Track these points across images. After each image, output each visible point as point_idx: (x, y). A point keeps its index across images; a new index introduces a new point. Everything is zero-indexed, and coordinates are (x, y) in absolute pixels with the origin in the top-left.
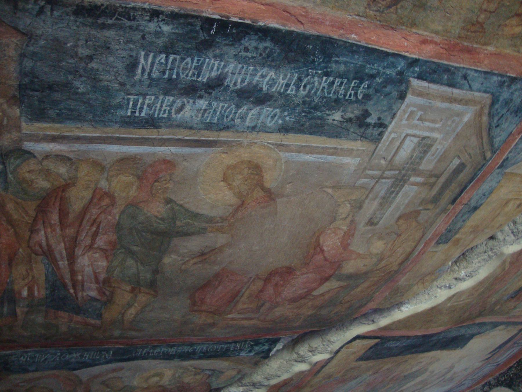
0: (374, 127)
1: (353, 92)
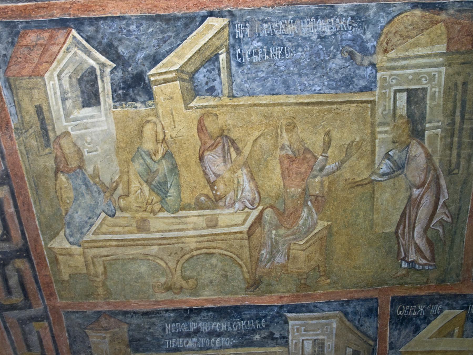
0: (281, 339)
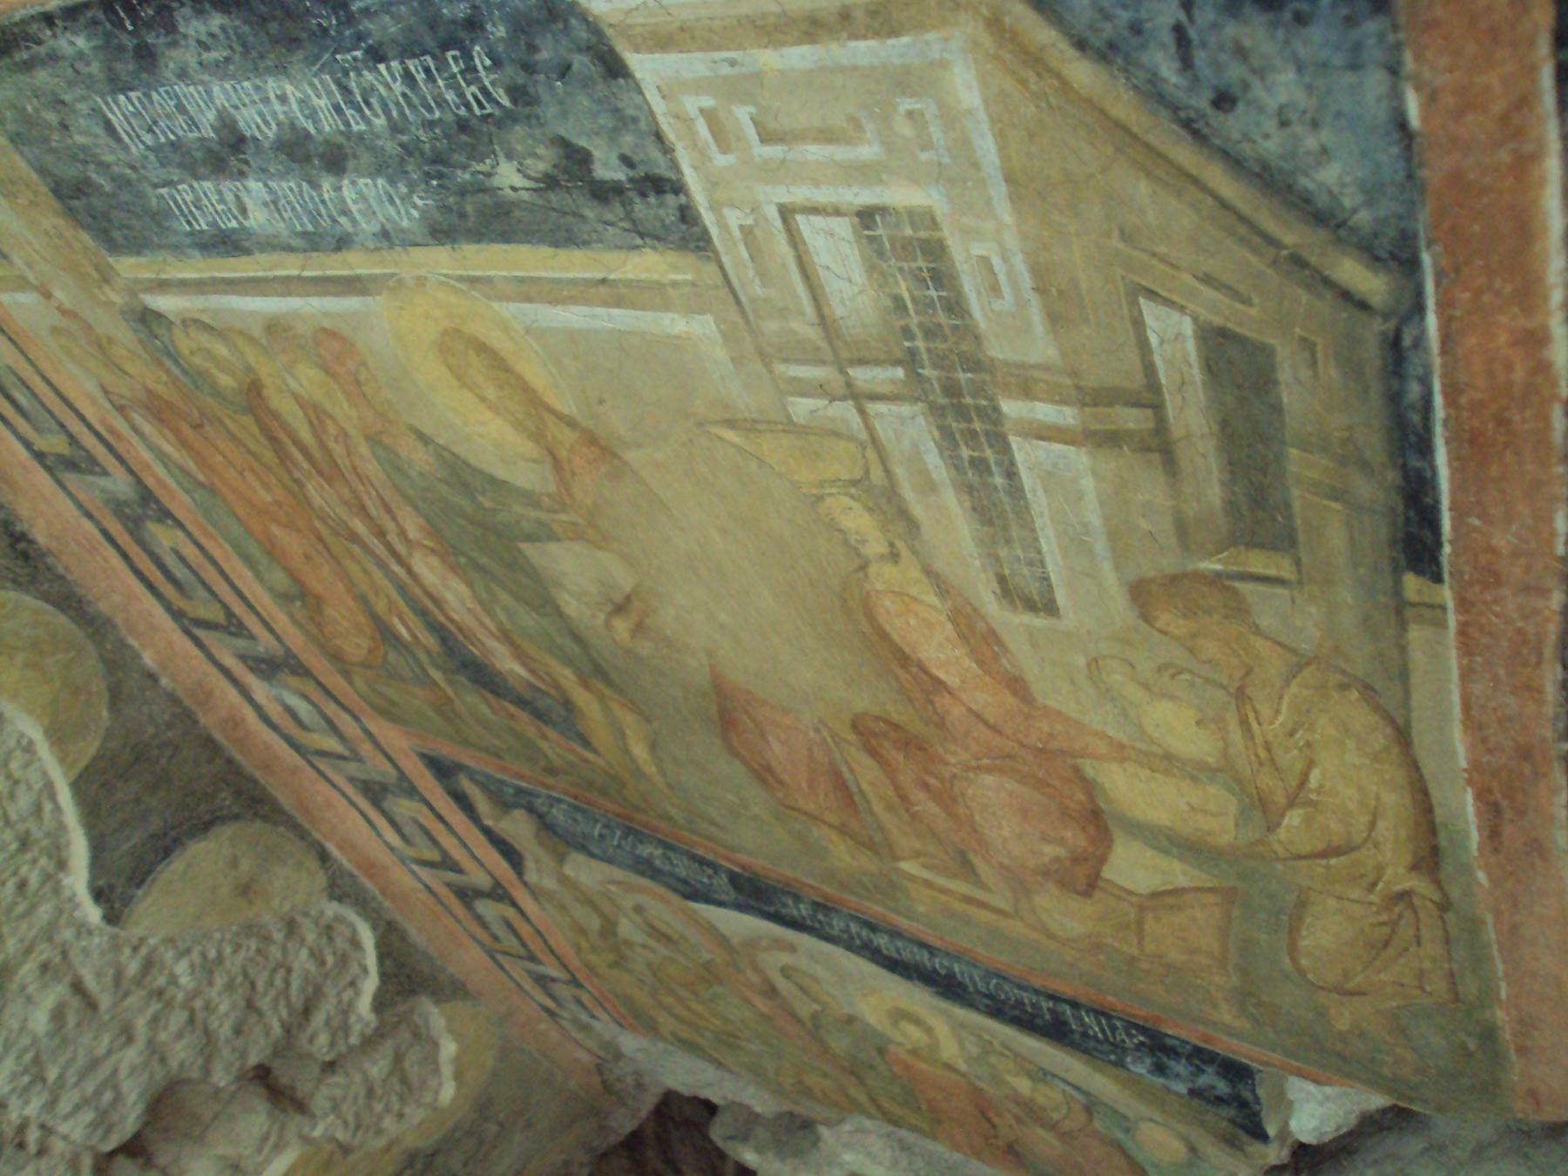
1: (474, 89)
